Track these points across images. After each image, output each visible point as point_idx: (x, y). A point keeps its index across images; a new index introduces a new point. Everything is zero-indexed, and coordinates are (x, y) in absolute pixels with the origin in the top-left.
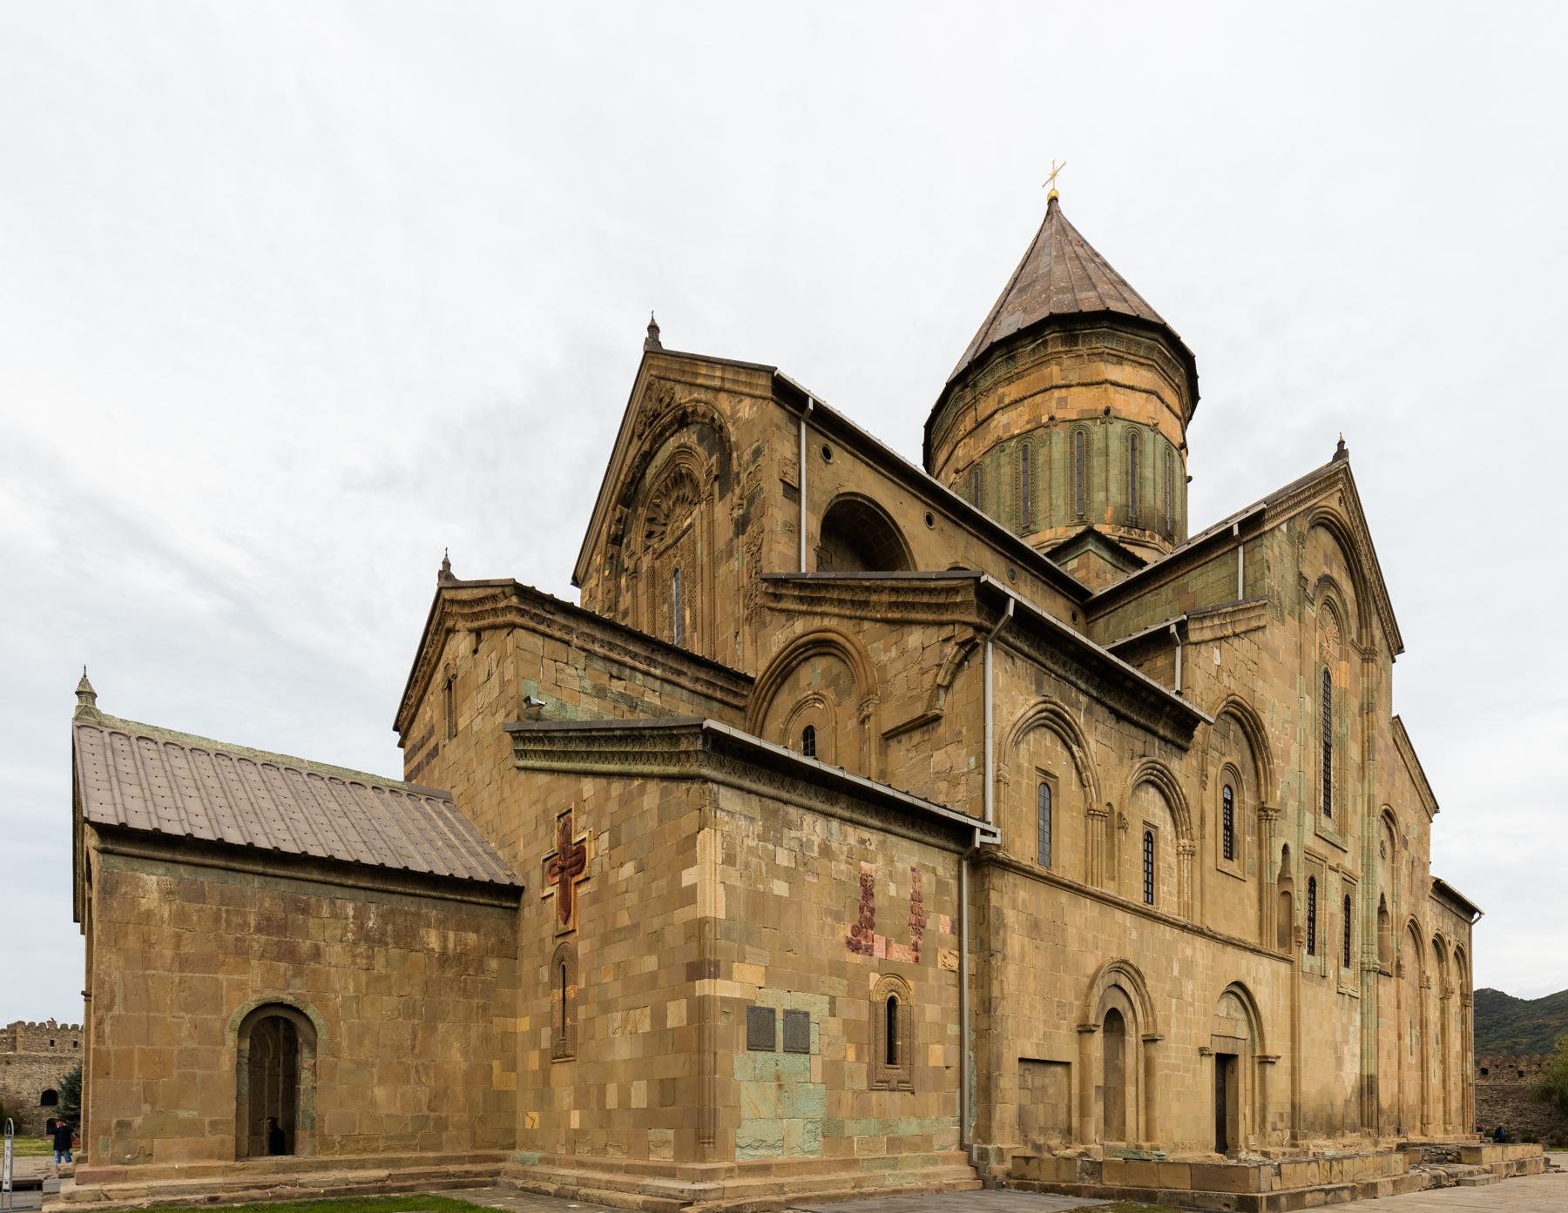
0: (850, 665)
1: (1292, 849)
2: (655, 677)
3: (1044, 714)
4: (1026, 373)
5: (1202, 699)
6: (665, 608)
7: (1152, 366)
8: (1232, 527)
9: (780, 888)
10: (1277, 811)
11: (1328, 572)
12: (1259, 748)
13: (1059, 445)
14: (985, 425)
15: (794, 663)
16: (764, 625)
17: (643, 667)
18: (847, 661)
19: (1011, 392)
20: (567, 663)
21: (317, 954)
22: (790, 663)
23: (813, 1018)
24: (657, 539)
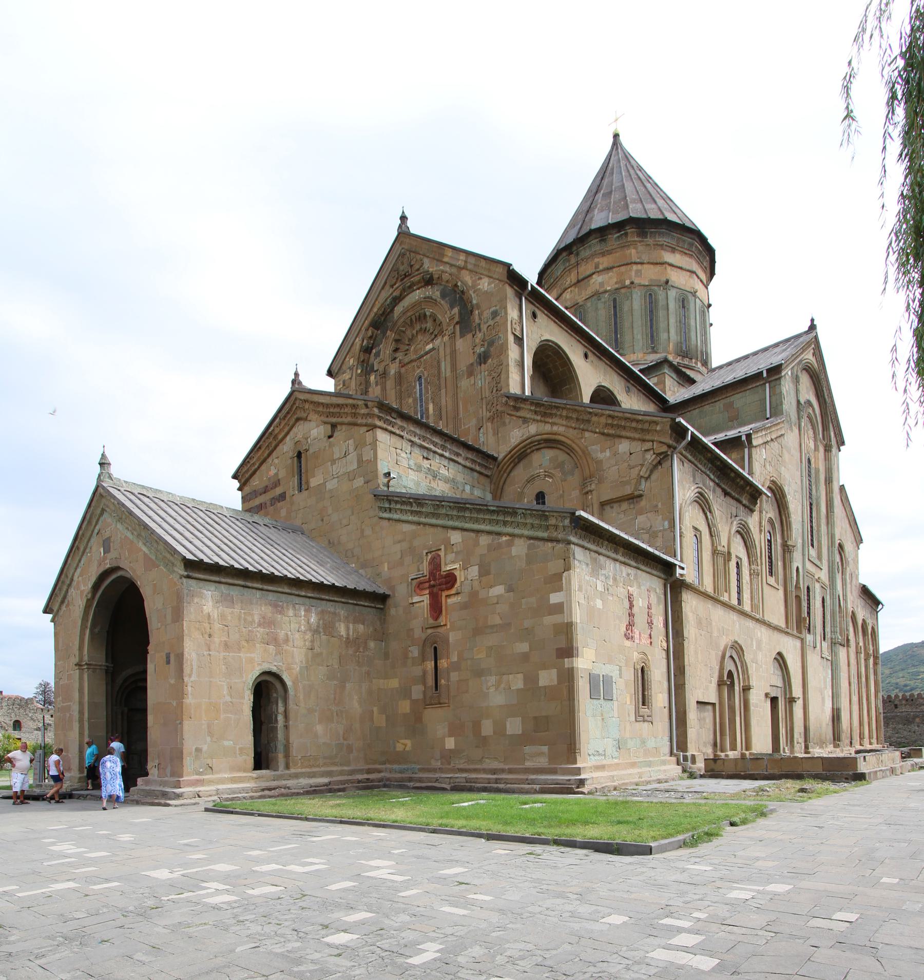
0: (573, 456)
1: (801, 570)
2: (446, 458)
3: (697, 495)
4: (614, 251)
5: (759, 479)
6: (411, 400)
7: (692, 255)
8: (762, 371)
9: (599, 604)
10: (794, 546)
11: (808, 398)
12: (784, 509)
13: (637, 302)
14: (586, 280)
15: (529, 451)
16: (504, 424)
17: (440, 451)
18: (571, 454)
19: (604, 262)
20: (402, 450)
21: (287, 640)
22: (526, 450)
23: (614, 679)
24: (401, 354)
